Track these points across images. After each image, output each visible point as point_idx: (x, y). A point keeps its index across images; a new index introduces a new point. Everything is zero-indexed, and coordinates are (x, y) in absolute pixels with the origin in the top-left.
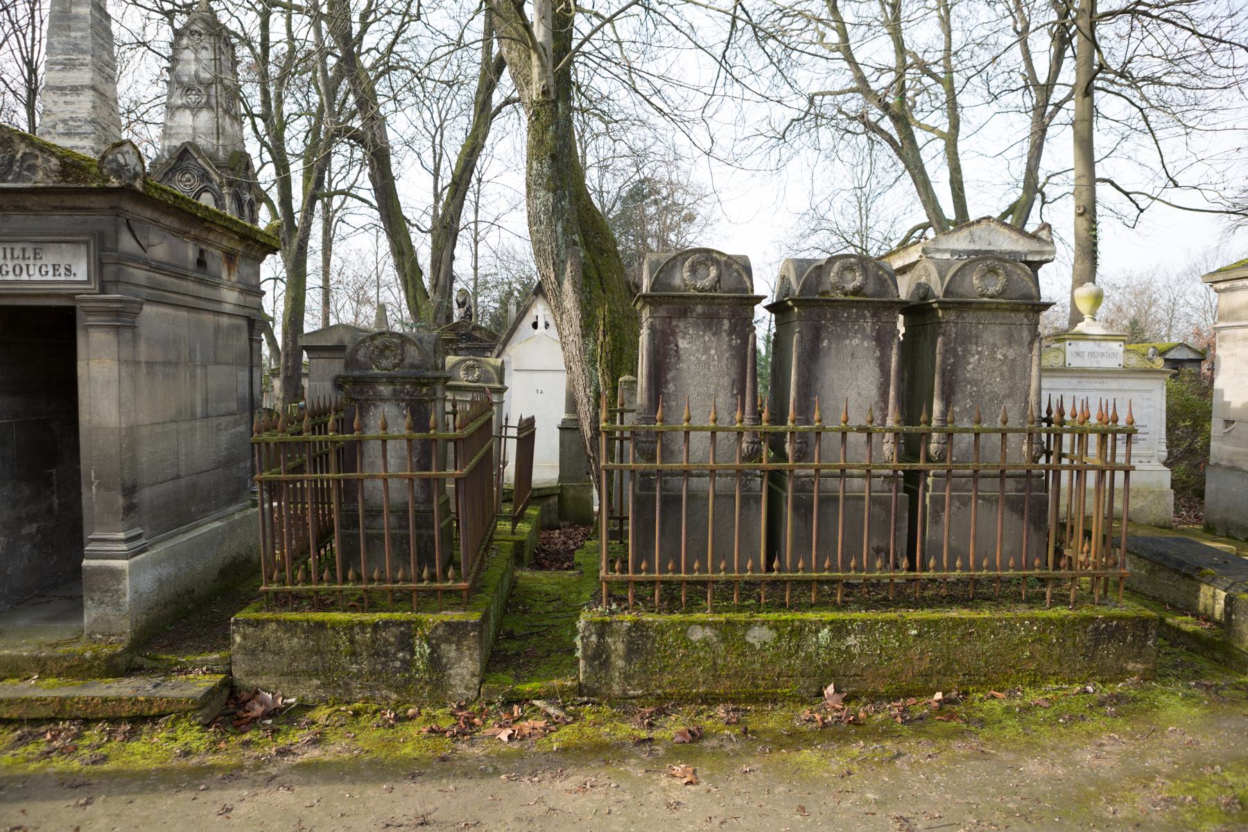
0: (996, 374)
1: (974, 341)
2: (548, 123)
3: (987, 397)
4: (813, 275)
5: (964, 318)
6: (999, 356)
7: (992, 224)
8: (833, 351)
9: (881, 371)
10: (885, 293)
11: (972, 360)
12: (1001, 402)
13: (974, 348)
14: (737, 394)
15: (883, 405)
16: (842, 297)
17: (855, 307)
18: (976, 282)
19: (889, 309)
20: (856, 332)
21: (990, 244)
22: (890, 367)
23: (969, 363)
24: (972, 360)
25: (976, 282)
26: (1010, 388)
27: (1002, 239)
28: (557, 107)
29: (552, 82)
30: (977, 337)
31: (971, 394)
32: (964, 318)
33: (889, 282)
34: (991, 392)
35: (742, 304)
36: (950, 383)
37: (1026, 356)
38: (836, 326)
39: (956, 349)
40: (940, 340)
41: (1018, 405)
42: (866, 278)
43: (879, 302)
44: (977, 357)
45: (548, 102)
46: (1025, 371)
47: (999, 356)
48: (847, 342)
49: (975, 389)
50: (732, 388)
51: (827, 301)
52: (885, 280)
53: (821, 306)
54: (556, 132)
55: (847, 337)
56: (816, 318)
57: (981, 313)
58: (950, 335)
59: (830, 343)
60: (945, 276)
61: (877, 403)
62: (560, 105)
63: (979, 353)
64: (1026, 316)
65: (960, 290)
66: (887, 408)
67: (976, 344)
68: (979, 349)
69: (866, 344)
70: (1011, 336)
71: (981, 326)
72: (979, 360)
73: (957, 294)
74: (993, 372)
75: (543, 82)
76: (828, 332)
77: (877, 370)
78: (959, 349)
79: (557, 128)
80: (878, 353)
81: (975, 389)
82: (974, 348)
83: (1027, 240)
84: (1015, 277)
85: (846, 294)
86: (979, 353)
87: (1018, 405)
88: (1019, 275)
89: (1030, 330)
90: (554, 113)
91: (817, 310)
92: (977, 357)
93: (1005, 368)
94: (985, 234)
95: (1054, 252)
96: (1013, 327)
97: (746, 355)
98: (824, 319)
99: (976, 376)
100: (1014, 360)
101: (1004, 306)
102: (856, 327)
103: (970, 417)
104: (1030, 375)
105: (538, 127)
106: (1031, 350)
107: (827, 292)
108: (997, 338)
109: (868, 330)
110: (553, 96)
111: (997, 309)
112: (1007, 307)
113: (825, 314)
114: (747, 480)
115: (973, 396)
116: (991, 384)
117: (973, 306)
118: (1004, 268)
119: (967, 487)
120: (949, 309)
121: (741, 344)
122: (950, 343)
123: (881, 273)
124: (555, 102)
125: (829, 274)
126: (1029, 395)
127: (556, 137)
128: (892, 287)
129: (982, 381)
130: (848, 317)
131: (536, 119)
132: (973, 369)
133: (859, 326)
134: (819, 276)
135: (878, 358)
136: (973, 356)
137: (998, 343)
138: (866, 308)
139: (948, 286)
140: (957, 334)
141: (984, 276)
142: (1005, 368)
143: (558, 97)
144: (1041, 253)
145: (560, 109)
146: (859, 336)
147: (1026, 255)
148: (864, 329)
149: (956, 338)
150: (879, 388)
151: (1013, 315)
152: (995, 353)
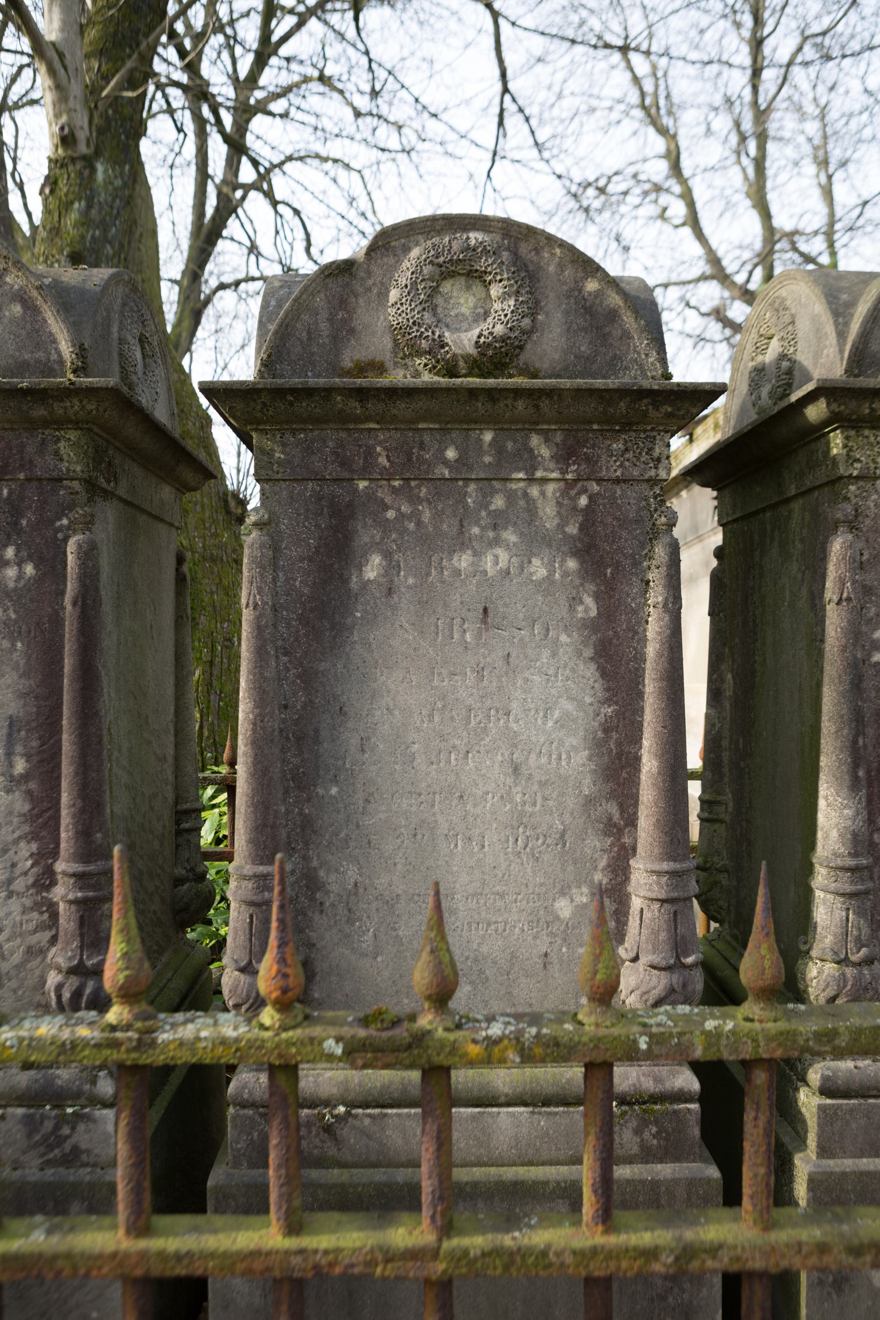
2: (71, 197)
4: (319, 301)
8: (405, 600)
9: (604, 673)
10: (614, 365)
14: (25, 777)
15: (613, 809)
16: (444, 381)
17: (492, 421)
19: (627, 426)
20: (498, 521)
22: (641, 658)
28: (93, 170)
29: (82, 120)
33: (628, 320)
35: (33, 425)
38: (415, 500)
40: (837, 546)
42: (533, 308)
43: (580, 393)
45: (73, 160)
48: (464, 561)
50: (9, 754)
51: (362, 394)
52: (613, 315)
53: (344, 419)
54: (86, 213)
55: (462, 542)
56: (332, 470)
59: (391, 567)
60: (852, 304)
61: (589, 802)
62: (100, 168)
66: (632, 822)
69: (538, 569)
75: (64, 119)
76: (385, 526)
77: (590, 671)
79: (89, 207)
80: (589, 606)
85: (451, 371)
90: (86, 181)
91: (332, 437)
97: (57, 621)
98: (365, 473)
102: (498, 502)
105: (53, 204)
107: (380, 368)
109: (548, 513)
110: (83, 148)
113: (370, 454)
114: (62, 1120)
121: (39, 580)
123: (592, 286)
124: (89, 162)
125: (384, 294)
127: (85, 221)
128: (641, 343)
130: (462, 461)
131: (52, 192)
133: (511, 498)
134: (343, 303)
135: (592, 626)
138: (533, 424)
139: (865, 335)
143: (98, 153)
145: (100, 175)
146: (510, 536)
148: (532, 510)
150: (598, 746)
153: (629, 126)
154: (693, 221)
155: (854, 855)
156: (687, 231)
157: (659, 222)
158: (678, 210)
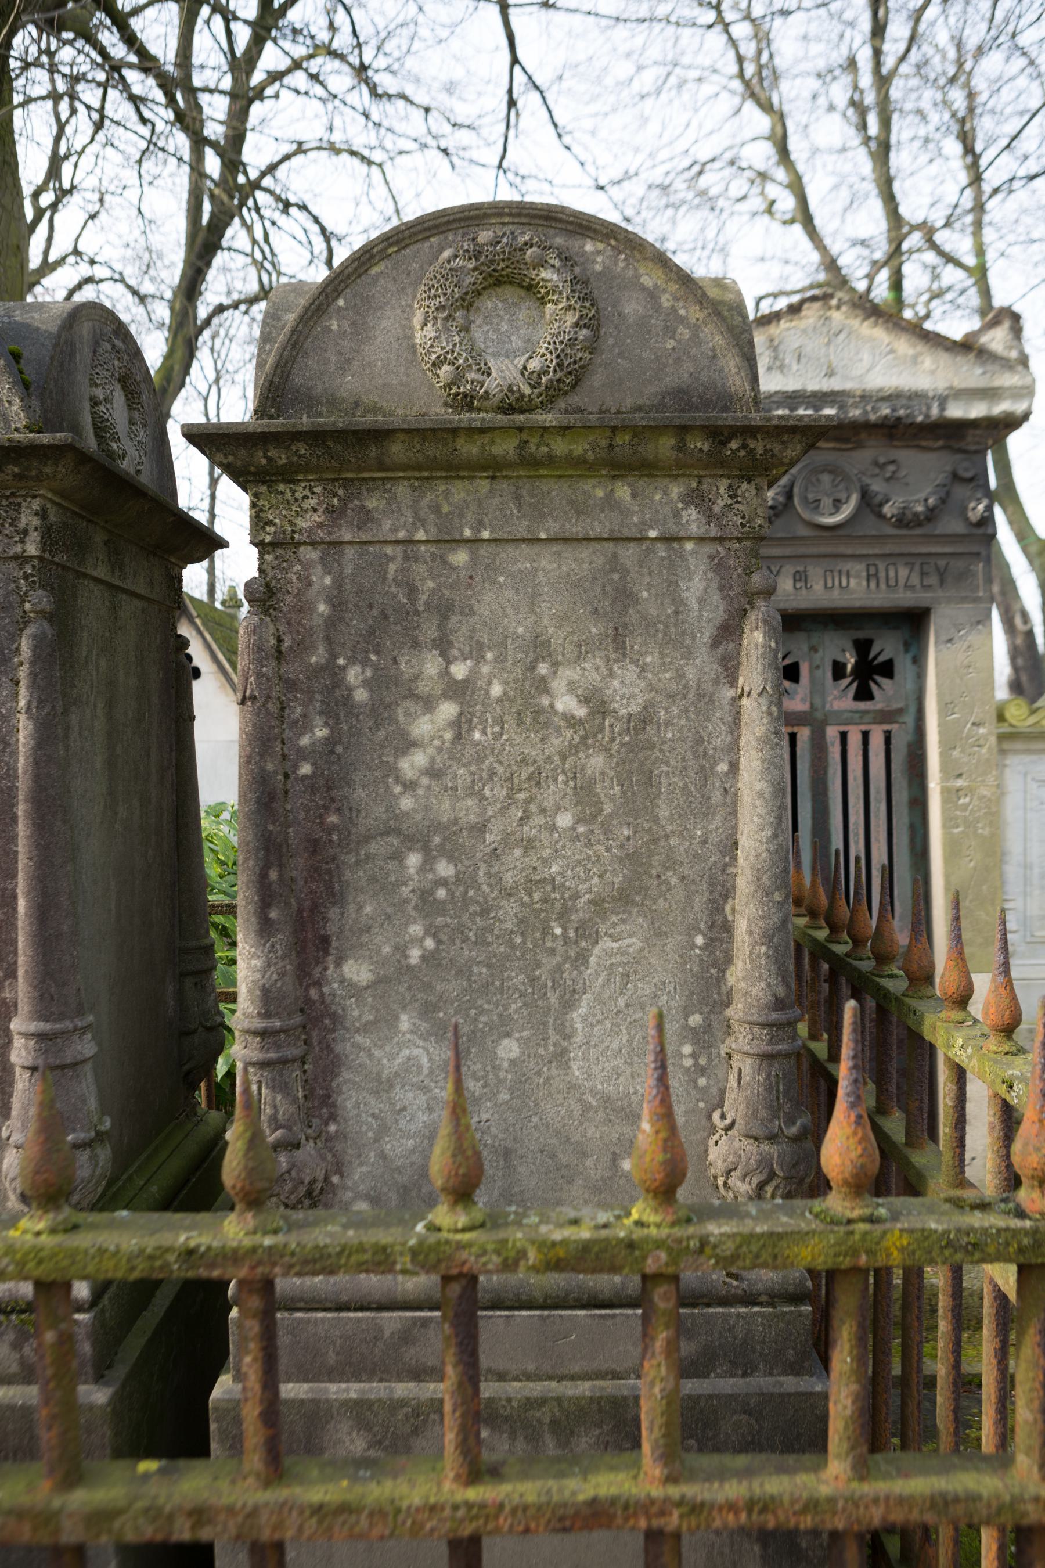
0: (550, 795)
1: (429, 630)
3: (510, 909)
5: (366, 518)
6: (566, 703)
7: (837, 316)
11: (423, 727)
12: (588, 932)
13: (432, 665)
18: (423, 335)
21: (830, 374)
23: (408, 745)
24: (423, 727)
25: (423, 335)
26: (631, 858)
27: (866, 357)
30: (444, 610)
31: (425, 895)
32: (366, 518)
34: (531, 884)
36: (314, 846)
37: (705, 701)
39: (334, 675)
41: (674, 942)
44: (448, 710)
46: (705, 773)
47: (566, 703)
49: (444, 869)
57: (459, 492)
58: (304, 608)
63: (456, 690)
64: (697, 498)
65: (349, 384)
67: (443, 646)
68: (459, 671)
70: (625, 597)
71: (460, 557)
72: (460, 726)
73: (333, 403)
74: (536, 780)
78: (353, 675)
81: (444, 869)
82: (432, 665)
83: (944, 357)
84: (632, 307)
86: (456, 690)
87: (674, 942)
88: (652, 295)
89: (719, 567)
92: (448, 710)
93: (596, 762)
94: (814, 345)
95: (1028, 391)
96: (629, 554)
99: (445, 809)
100: (644, 720)
101: (560, 447)
103: (428, 1010)
104: (731, 795)
106: (730, 667)
108: (547, 610)
111: (531, 463)
112: (579, 448)
115: (440, 908)
116: (529, 845)
117: (397, 449)
118: (567, 259)
119: (411, 1354)
120: (288, 475)
122: (303, 646)
126: (728, 893)
129: (480, 829)
132: (433, 772)
136: (429, 705)
137: (557, 637)
140: (337, 604)
141: (467, 302)
142: (596, 762)
144: (989, 394)
147: (943, 401)
149: (332, 623)
151: (623, 492)
152: (543, 686)
153: (728, 102)
154: (805, 218)
155: (266, 1015)
156: (797, 229)
157: (766, 218)
158: (787, 203)
